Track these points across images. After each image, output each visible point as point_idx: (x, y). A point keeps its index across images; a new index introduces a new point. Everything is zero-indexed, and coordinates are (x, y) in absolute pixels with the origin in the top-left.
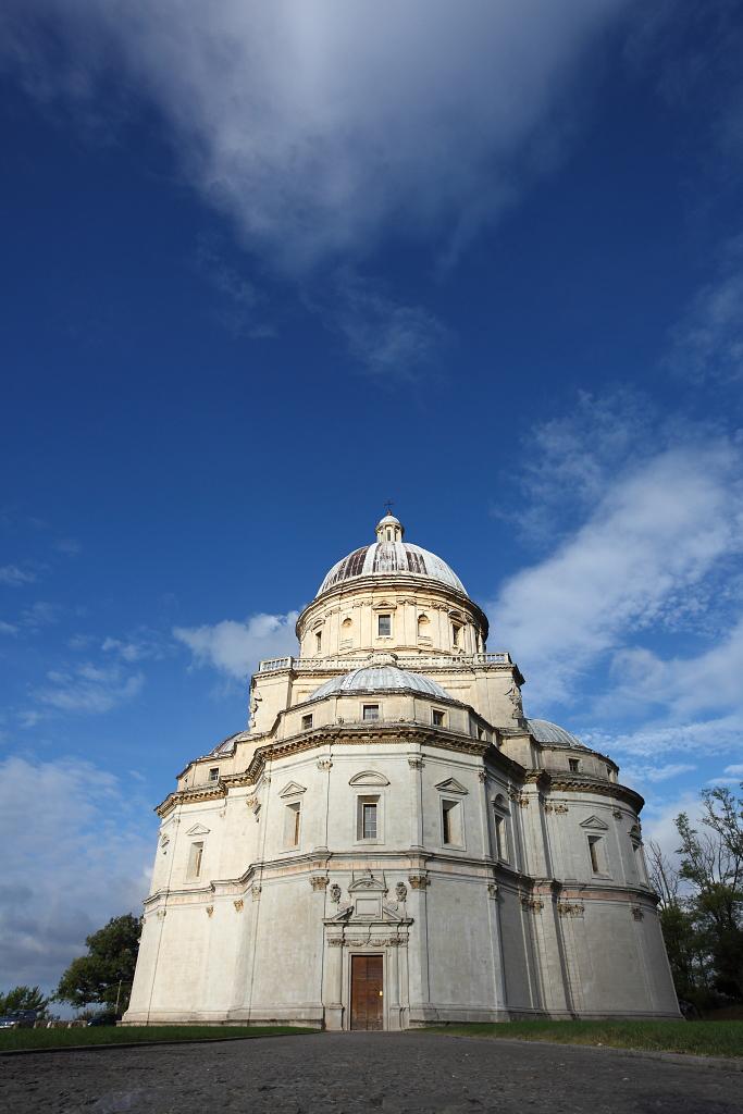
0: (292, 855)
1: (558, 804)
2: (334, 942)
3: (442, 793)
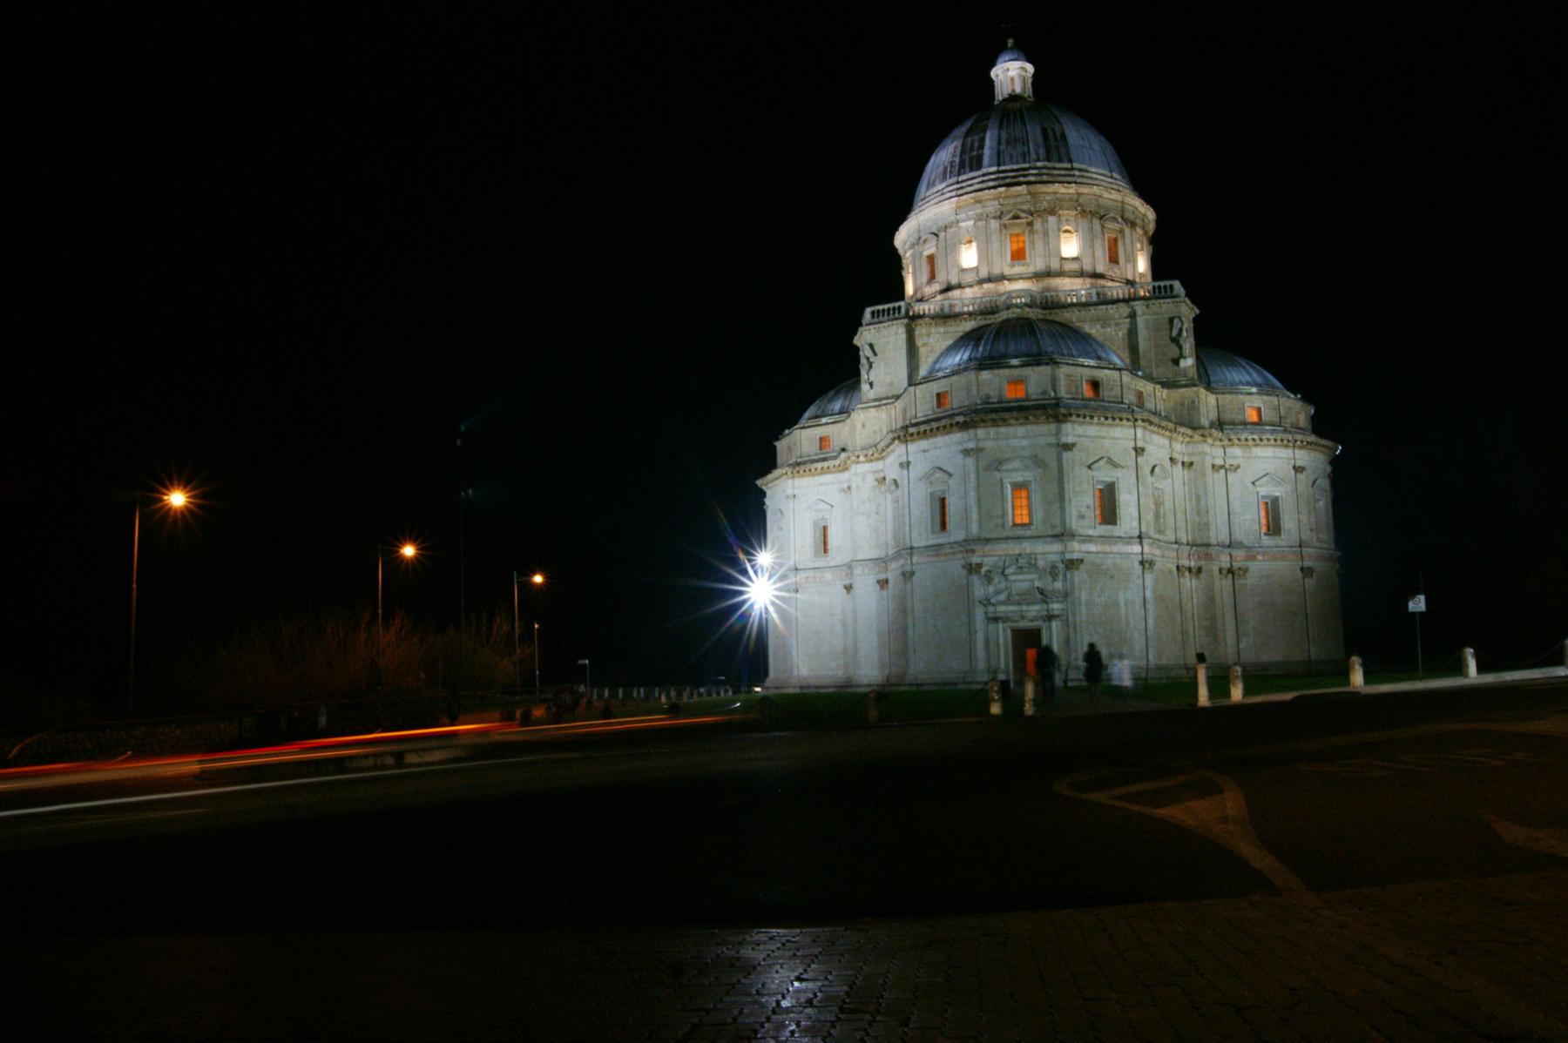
0: (943, 540)
1: (1229, 462)
2: (996, 619)
3: (1095, 473)
